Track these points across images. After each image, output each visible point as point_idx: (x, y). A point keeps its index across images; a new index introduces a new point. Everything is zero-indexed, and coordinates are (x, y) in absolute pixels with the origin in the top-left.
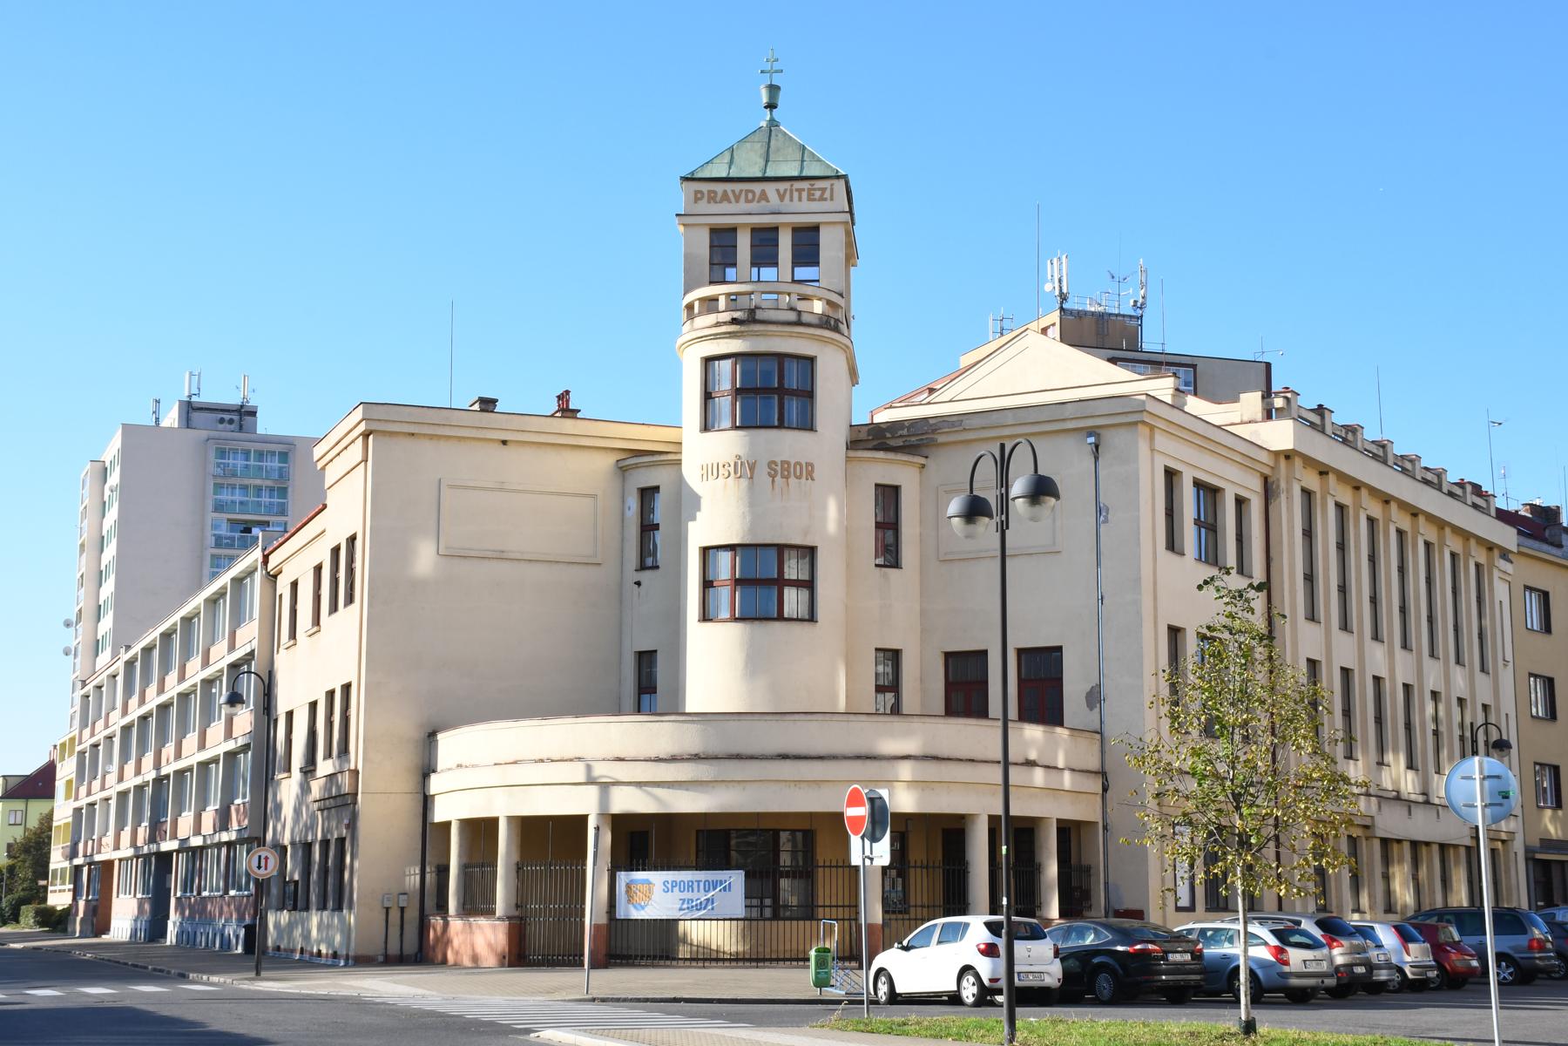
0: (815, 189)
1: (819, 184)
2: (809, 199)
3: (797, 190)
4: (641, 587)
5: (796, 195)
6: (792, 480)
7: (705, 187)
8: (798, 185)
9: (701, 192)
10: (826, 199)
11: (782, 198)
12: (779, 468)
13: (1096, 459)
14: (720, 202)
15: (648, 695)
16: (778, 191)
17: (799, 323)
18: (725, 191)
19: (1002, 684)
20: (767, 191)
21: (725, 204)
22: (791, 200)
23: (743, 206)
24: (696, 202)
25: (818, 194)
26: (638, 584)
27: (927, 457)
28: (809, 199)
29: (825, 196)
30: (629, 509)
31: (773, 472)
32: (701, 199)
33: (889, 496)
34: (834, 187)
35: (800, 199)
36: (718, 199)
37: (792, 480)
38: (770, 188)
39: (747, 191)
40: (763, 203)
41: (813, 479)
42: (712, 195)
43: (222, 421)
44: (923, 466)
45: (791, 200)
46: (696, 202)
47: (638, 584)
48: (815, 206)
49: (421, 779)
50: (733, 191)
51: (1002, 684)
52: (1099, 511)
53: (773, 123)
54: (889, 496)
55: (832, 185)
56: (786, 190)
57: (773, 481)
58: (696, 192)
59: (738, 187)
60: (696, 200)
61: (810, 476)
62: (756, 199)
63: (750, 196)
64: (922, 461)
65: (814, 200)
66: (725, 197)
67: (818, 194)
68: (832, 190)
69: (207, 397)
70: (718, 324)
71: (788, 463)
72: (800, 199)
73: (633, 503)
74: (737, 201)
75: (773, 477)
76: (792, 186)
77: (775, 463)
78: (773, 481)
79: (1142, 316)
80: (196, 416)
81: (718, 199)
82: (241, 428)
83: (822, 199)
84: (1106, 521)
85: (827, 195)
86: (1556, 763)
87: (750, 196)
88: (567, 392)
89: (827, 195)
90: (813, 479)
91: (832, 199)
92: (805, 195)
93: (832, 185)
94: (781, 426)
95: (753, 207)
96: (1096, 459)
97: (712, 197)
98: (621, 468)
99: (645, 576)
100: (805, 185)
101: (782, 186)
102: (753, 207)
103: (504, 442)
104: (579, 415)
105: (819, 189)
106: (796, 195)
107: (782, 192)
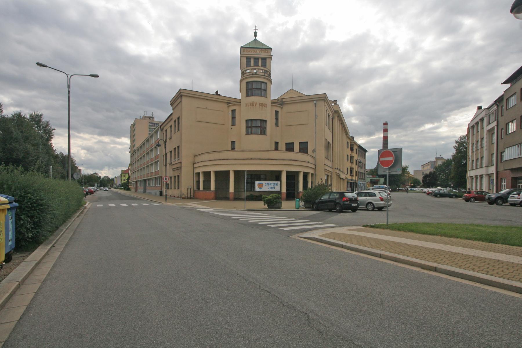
1: (267, 50)
5: (262, 51)
6: (263, 107)
8: (263, 50)
11: (260, 52)
12: (261, 104)
17: (264, 76)
19: (297, 147)
21: (249, 53)
22: (261, 52)
23: (252, 53)
25: (266, 52)
26: (232, 128)
33: (277, 112)
35: (263, 52)
36: (248, 51)
37: (263, 107)
38: (258, 50)
43: (149, 119)
45: (261, 52)
47: (232, 128)
51: (297, 147)
52: (316, 116)
53: (255, 40)
54: (277, 112)
57: (260, 107)
59: (251, 49)
61: (266, 106)
64: (282, 107)
66: (249, 51)
69: (147, 115)
72: (263, 52)
73: (230, 113)
74: (251, 52)
75: (260, 106)
77: (260, 103)
80: (146, 118)
81: (248, 51)
82: (152, 120)
83: (267, 53)
84: (317, 118)
85: (268, 52)
88: (218, 91)
89: (268, 52)
92: (264, 52)
94: (261, 96)
95: (255, 53)
99: (233, 127)
100: (264, 50)
101: (260, 50)
102: (255, 53)
103: (207, 99)
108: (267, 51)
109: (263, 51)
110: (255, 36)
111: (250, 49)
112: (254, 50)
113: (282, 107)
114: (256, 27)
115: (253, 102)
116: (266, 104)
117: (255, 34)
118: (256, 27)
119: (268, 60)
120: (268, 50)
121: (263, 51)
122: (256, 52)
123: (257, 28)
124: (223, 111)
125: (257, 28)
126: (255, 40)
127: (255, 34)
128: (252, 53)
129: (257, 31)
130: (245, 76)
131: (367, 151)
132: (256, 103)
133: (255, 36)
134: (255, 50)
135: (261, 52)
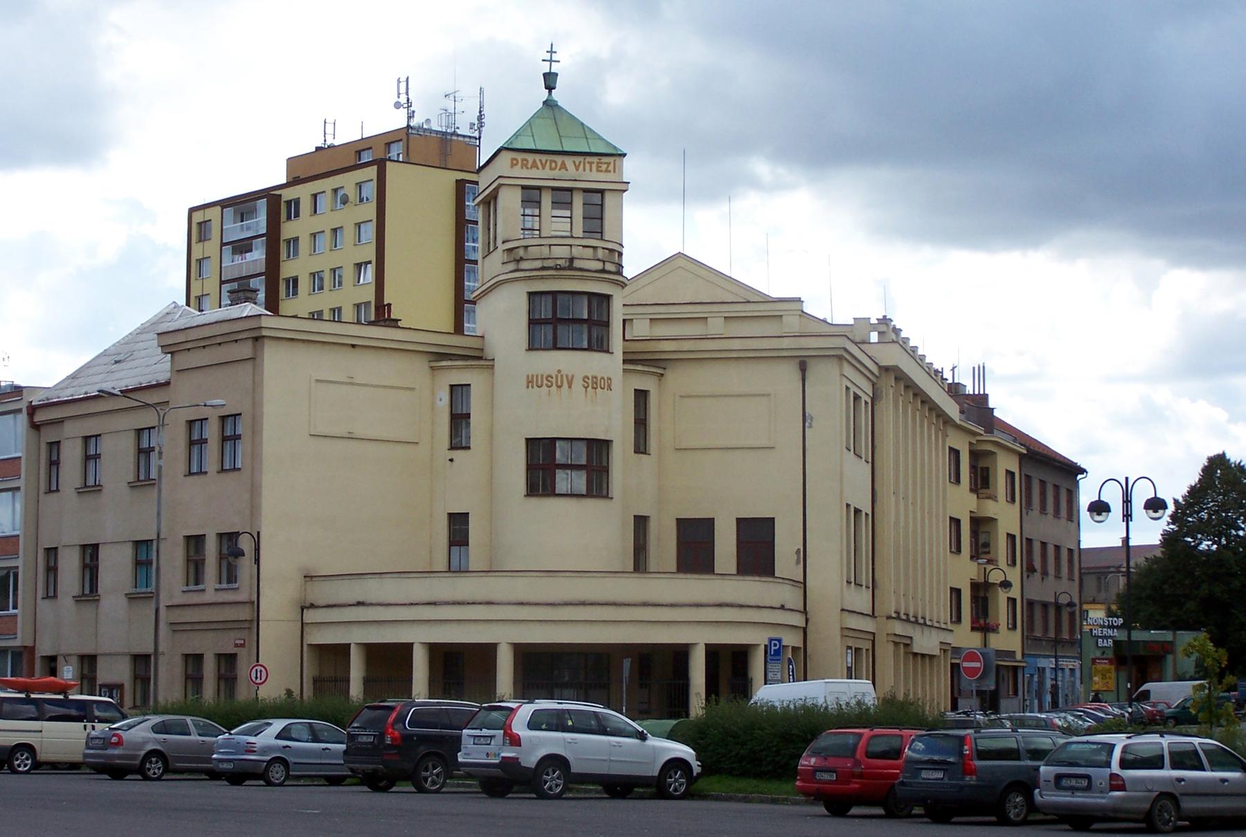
0: (601, 163)
1: (605, 159)
2: (598, 171)
3: (588, 163)
4: (454, 463)
5: (588, 166)
7: (519, 156)
8: (589, 159)
9: (516, 159)
10: (610, 171)
12: (590, 382)
13: (804, 380)
14: (531, 168)
15: (458, 548)
16: (574, 162)
17: (603, 271)
18: (534, 161)
20: (566, 163)
21: (535, 169)
22: (584, 170)
23: (547, 173)
24: (512, 167)
26: (451, 460)
27: (665, 369)
28: (598, 171)
29: (609, 169)
30: (441, 400)
31: (586, 385)
32: (516, 165)
34: (616, 162)
35: (591, 170)
38: (569, 161)
39: (551, 161)
40: (563, 170)
41: (611, 390)
42: (525, 162)
44: (662, 375)
45: (584, 170)
46: (512, 167)
47: (451, 460)
48: (602, 177)
49: (300, 610)
50: (541, 161)
54: (641, 397)
55: (615, 161)
56: (580, 162)
57: (586, 391)
58: (513, 159)
59: (544, 158)
60: (513, 165)
62: (558, 168)
63: (553, 165)
64: (660, 371)
65: (601, 171)
66: (534, 165)
67: (604, 167)
68: (615, 164)
70: (543, 268)
71: (596, 378)
72: (591, 170)
74: (543, 168)
75: (586, 388)
76: (585, 159)
78: (586, 391)
79: (480, 138)
83: (607, 171)
84: (810, 426)
85: (611, 168)
86: (958, 587)
87: (553, 165)
89: (611, 168)
90: (611, 390)
91: (614, 172)
92: (594, 167)
93: (615, 161)
96: (804, 380)
97: (524, 165)
98: (431, 367)
100: (595, 159)
101: (578, 159)
103: (353, 346)
104: (400, 324)
105: (605, 163)
106: (588, 166)
107: (577, 164)
108: (609, 164)
109: (591, 163)
110: (550, 87)
111: (538, 157)
112: (555, 162)
113: (660, 371)
114: (551, 52)
115: (559, 371)
116: (609, 379)
117: (550, 80)
118: (551, 52)
119: (609, 200)
120: (611, 160)
121: (591, 163)
122: (564, 166)
123: (555, 57)
124: (412, 389)
125: (555, 57)
126: (549, 104)
127: (550, 80)
128: (547, 173)
129: (555, 68)
130: (522, 270)
131: (1083, 471)
132: (573, 376)
133: (550, 87)
134: (559, 159)
135: (581, 167)
